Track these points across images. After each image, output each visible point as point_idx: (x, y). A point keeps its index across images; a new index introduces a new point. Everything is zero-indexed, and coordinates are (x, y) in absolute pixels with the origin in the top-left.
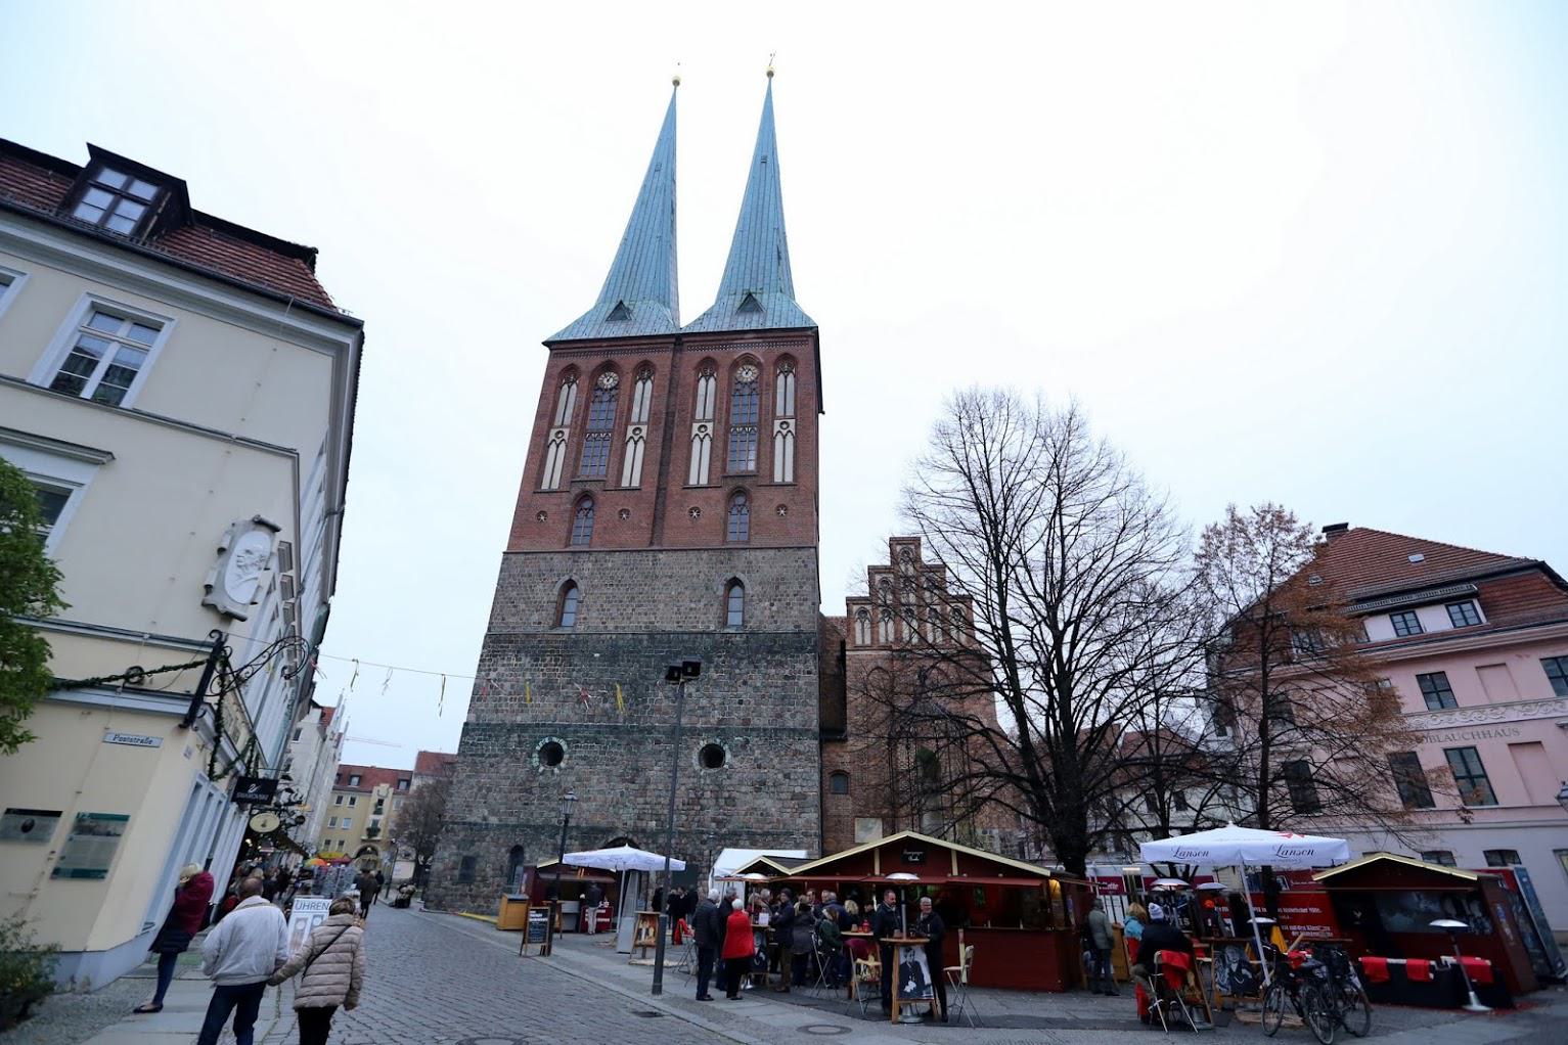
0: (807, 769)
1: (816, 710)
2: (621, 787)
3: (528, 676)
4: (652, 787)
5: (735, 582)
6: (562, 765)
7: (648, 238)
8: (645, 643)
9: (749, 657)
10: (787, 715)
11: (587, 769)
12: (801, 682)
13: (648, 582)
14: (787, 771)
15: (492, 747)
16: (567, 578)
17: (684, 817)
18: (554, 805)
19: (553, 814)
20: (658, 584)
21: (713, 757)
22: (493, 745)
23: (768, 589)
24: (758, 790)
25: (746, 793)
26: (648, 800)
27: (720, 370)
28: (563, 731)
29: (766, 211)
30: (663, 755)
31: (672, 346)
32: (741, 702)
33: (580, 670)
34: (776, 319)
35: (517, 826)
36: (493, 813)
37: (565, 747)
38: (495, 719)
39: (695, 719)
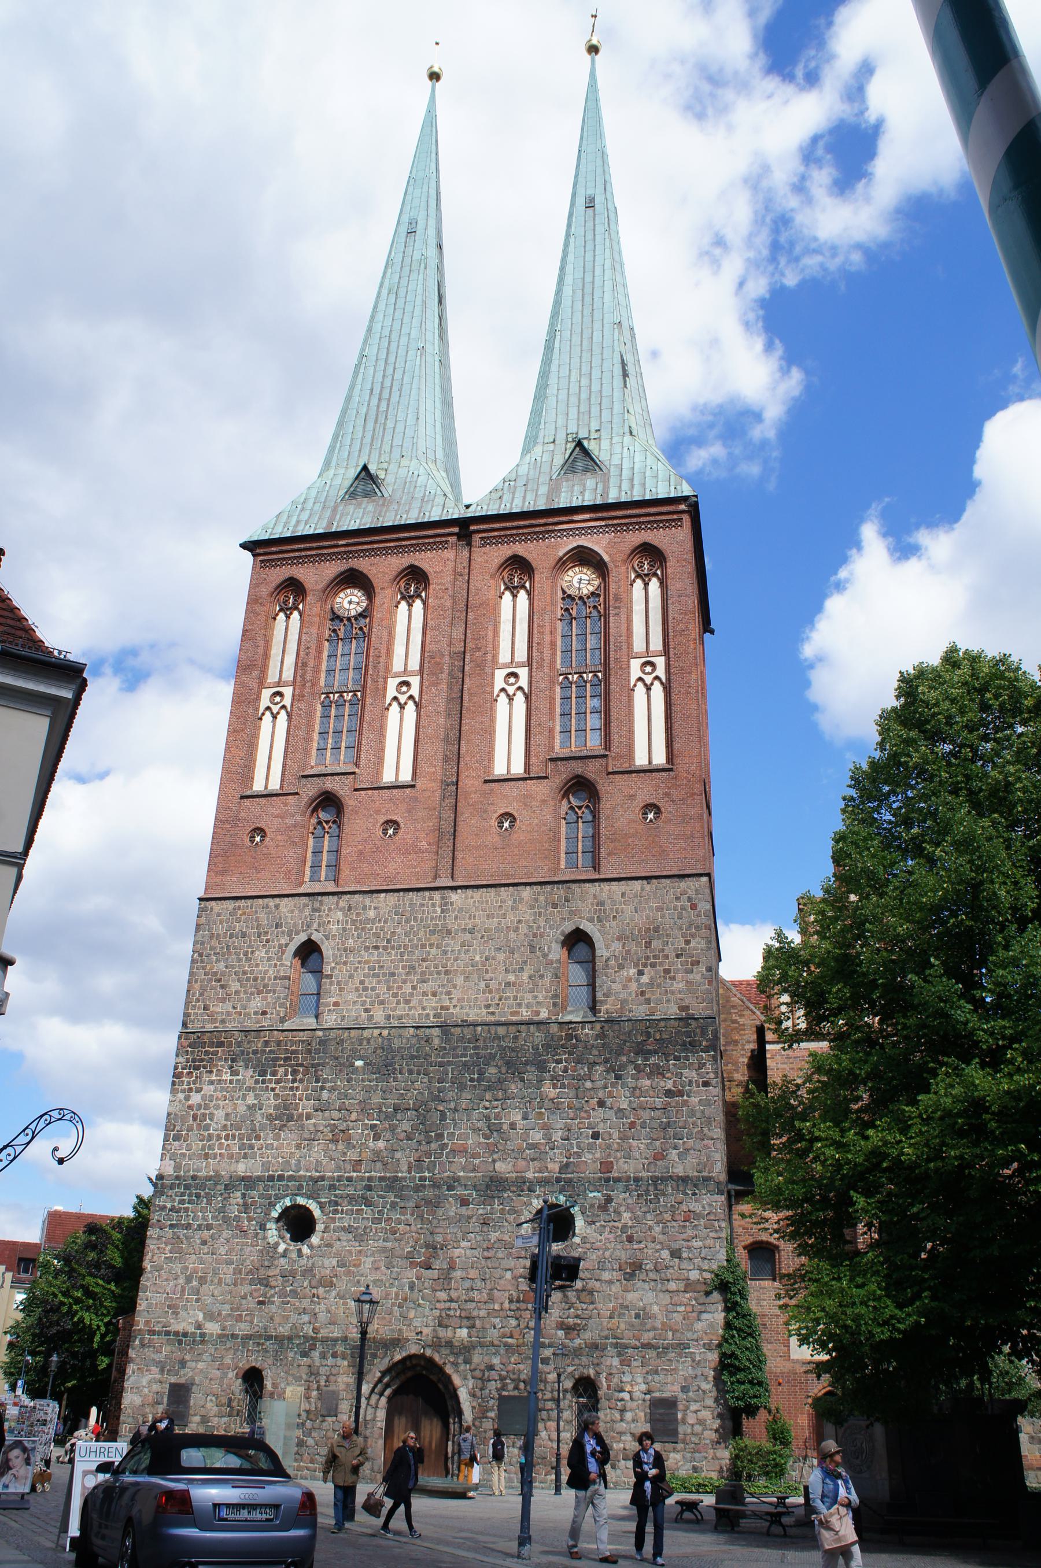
0: (709, 1242)
1: (721, 1146)
2: (411, 1274)
3: (251, 1100)
4: (458, 1274)
6: (315, 1240)
7: (402, 352)
8: (436, 1042)
9: (606, 1061)
10: (674, 1154)
11: (355, 1247)
12: (694, 1100)
13: (434, 939)
14: (675, 1246)
16: (303, 937)
17: (513, 1322)
18: (306, 1303)
19: (306, 1318)
20: (453, 944)
22: (204, 1210)
23: (633, 947)
24: (630, 1277)
25: (610, 1282)
26: (454, 1294)
27: (537, 577)
28: (314, 1186)
29: (597, 293)
30: (474, 1225)
31: (452, 539)
32: (596, 1136)
33: (332, 1089)
34: (625, 486)
35: (249, 1337)
36: (210, 1316)
37: (317, 1213)
38: (205, 1169)
39: (521, 1164)
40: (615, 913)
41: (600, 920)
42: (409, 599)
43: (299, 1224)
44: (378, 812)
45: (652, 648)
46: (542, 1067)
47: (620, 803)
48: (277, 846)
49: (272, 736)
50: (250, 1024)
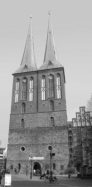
5: (52, 118)
15: (13, 148)
21: (50, 148)
40: (56, 115)
42: (31, 80)
43: (23, 149)
46: (48, 132)
47: (56, 103)
49: (17, 96)
50: (16, 128)
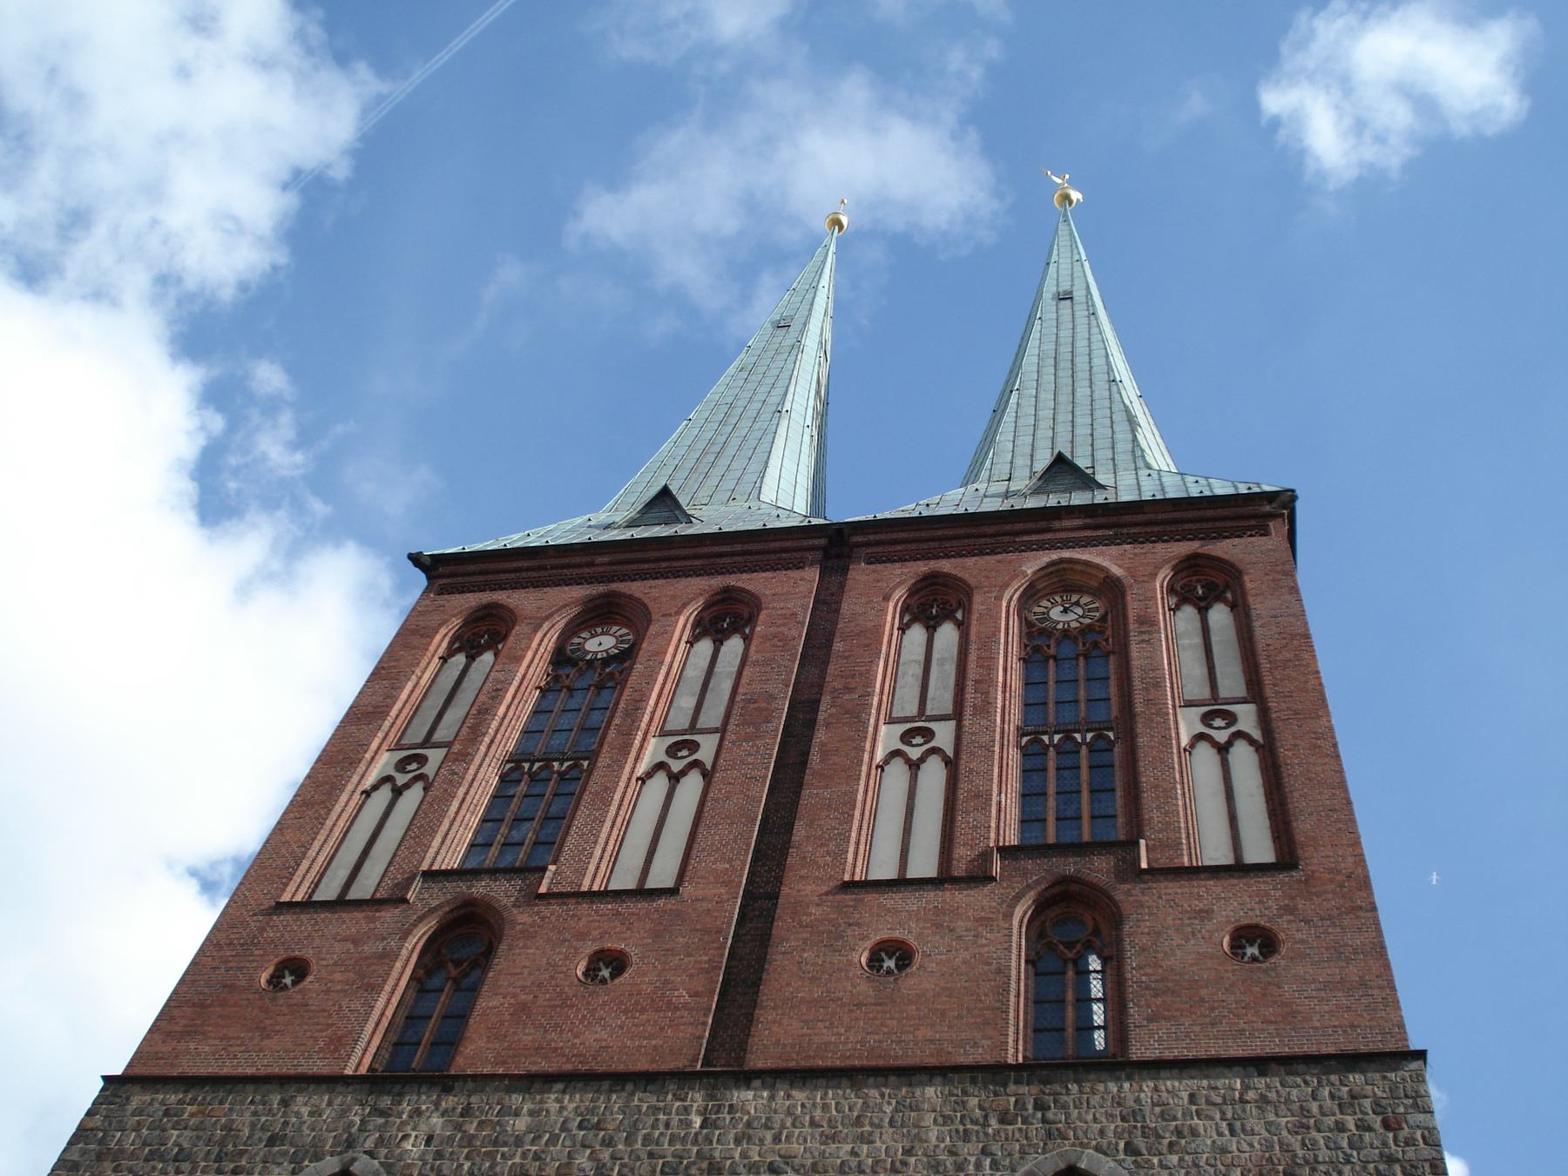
41: (1131, 1149)
44: (582, 936)
45: (1224, 693)
48: (328, 992)
